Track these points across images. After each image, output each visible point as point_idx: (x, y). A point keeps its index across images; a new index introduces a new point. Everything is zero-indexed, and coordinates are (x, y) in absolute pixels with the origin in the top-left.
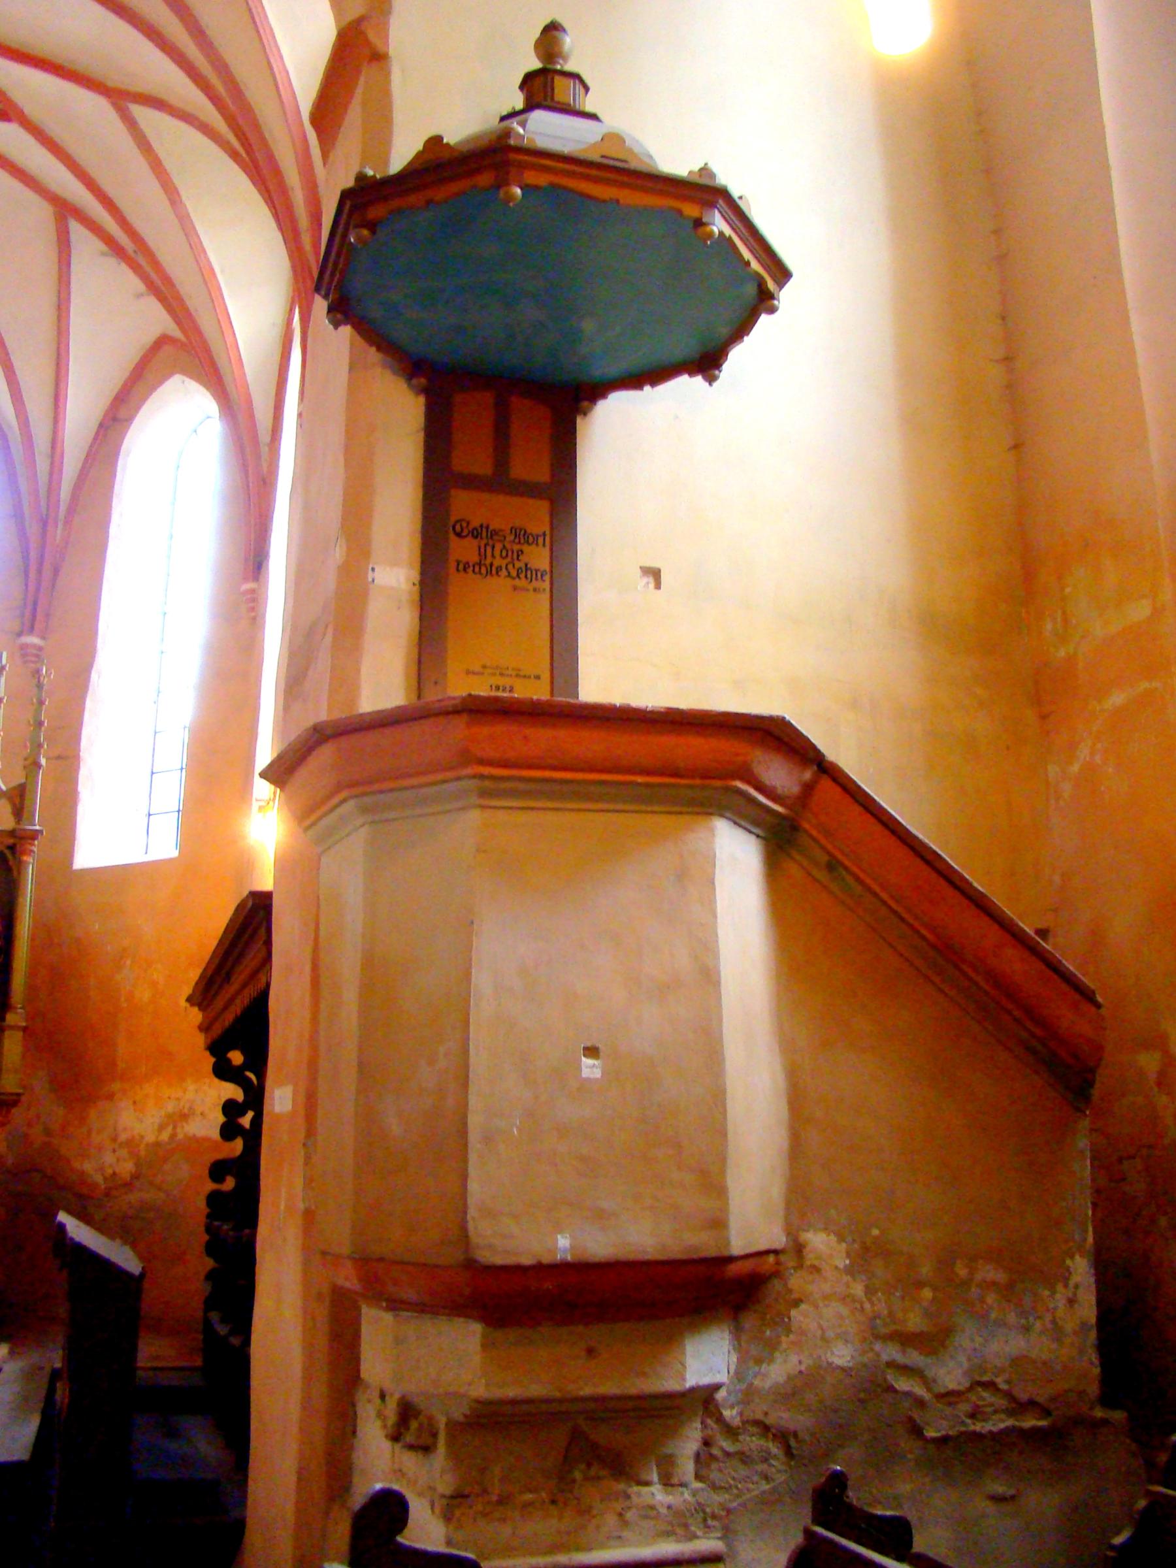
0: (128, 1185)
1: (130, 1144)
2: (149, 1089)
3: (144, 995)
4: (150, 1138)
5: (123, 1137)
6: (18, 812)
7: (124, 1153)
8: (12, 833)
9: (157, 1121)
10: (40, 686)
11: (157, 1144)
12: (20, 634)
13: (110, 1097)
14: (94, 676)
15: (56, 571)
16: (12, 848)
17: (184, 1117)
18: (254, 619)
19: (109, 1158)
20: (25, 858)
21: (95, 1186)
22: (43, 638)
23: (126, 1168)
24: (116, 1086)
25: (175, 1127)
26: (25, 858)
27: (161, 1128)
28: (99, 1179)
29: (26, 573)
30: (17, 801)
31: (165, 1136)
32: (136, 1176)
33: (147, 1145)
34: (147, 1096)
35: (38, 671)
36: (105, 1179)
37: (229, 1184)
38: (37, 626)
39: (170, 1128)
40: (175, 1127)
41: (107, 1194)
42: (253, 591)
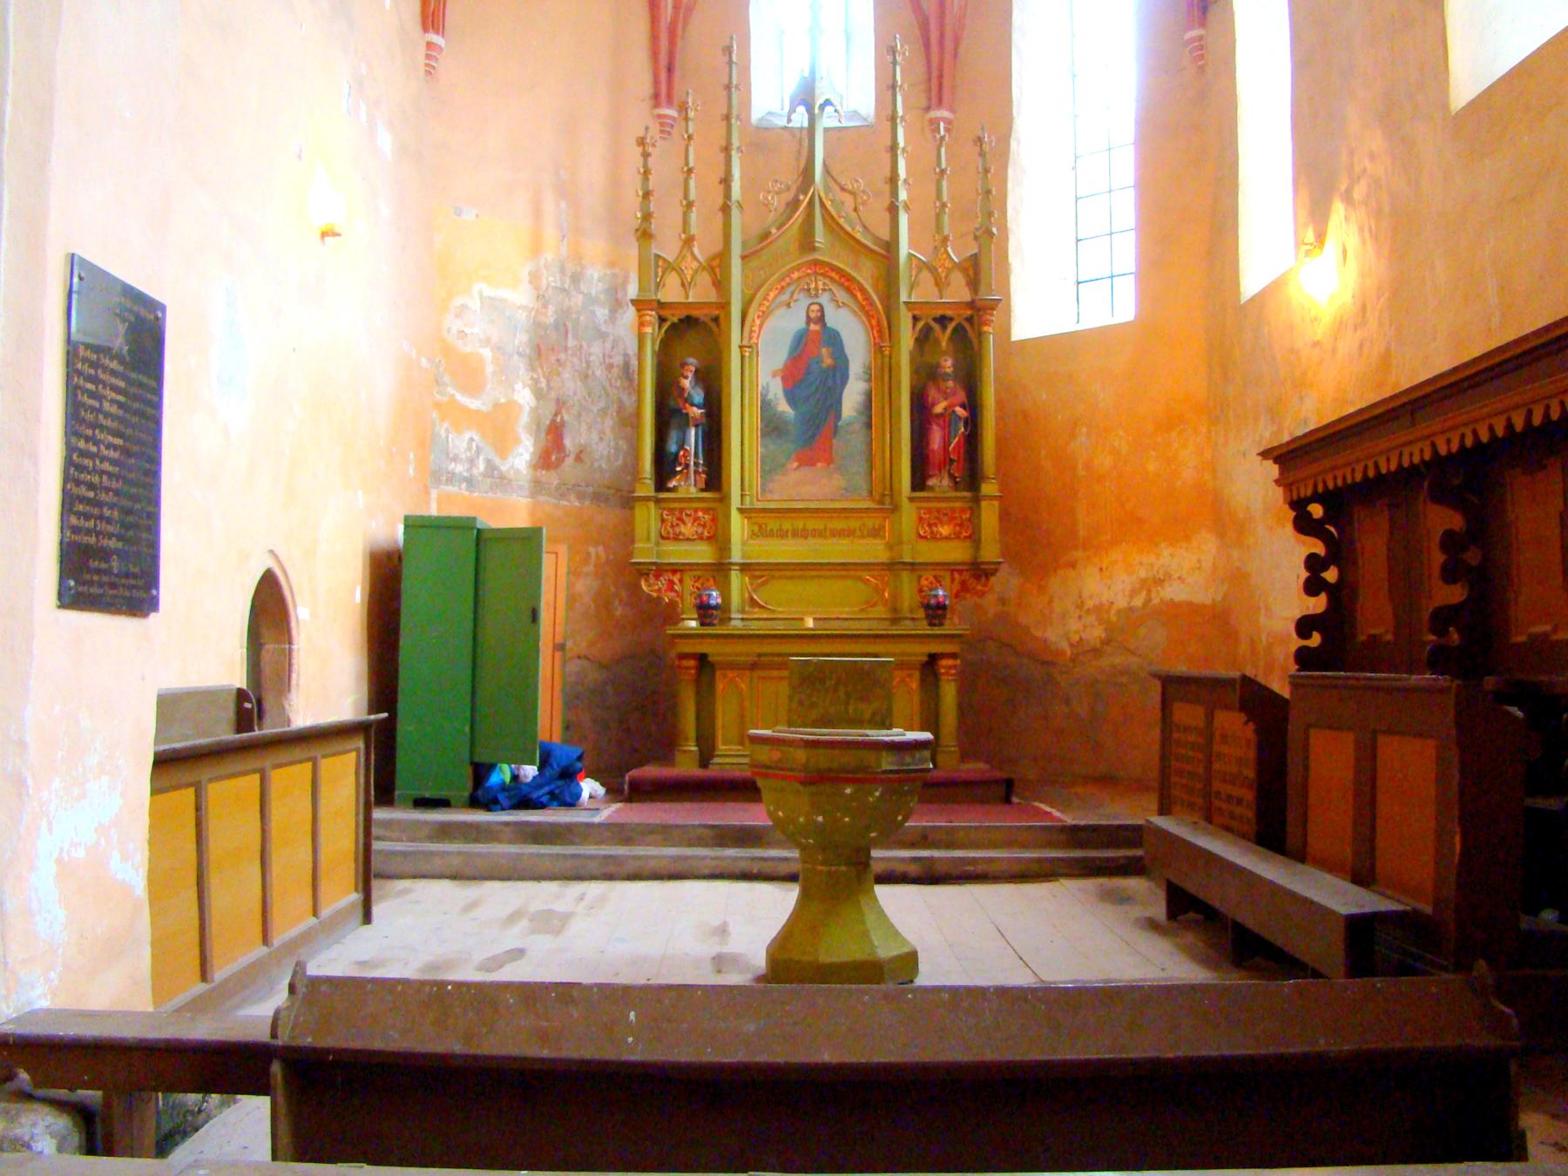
0: (1096, 652)
1: (1098, 609)
2: (1115, 554)
3: (1104, 462)
4: (1122, 603)
5: (1090, 604)
6: (974, 283)
7: (1091, 619)
8: (971, 305)
9: (1129, 588)
10: (982, 154)
11: (1131, 609)
12: (928, 109)
13: (1073, 565)
14: (1013, 143)
15: (957, 40)
16: (969, 320)
17: (1159, 582)
18: (1202, 68)
19: (1074, 625)
20: (985, 328)
21: (1060, 653)
22: (952, 111)
23: (1096, 633)
24: (1079, 554)
26: (985, 328)
27: (1133, 593)
28: (1065, 645)
29: (927, 46)
30: (971, 272)
31: (1138, 602)
32: (1107, 642)
33: (1119, 611)
34: (1114, 563)
35: (980, 140)
36: (1072, 645)
37: (1315, 640)
38: (946, 96)
40: (1149, 591)
41: (1072, 660)
42: (1201, 38)
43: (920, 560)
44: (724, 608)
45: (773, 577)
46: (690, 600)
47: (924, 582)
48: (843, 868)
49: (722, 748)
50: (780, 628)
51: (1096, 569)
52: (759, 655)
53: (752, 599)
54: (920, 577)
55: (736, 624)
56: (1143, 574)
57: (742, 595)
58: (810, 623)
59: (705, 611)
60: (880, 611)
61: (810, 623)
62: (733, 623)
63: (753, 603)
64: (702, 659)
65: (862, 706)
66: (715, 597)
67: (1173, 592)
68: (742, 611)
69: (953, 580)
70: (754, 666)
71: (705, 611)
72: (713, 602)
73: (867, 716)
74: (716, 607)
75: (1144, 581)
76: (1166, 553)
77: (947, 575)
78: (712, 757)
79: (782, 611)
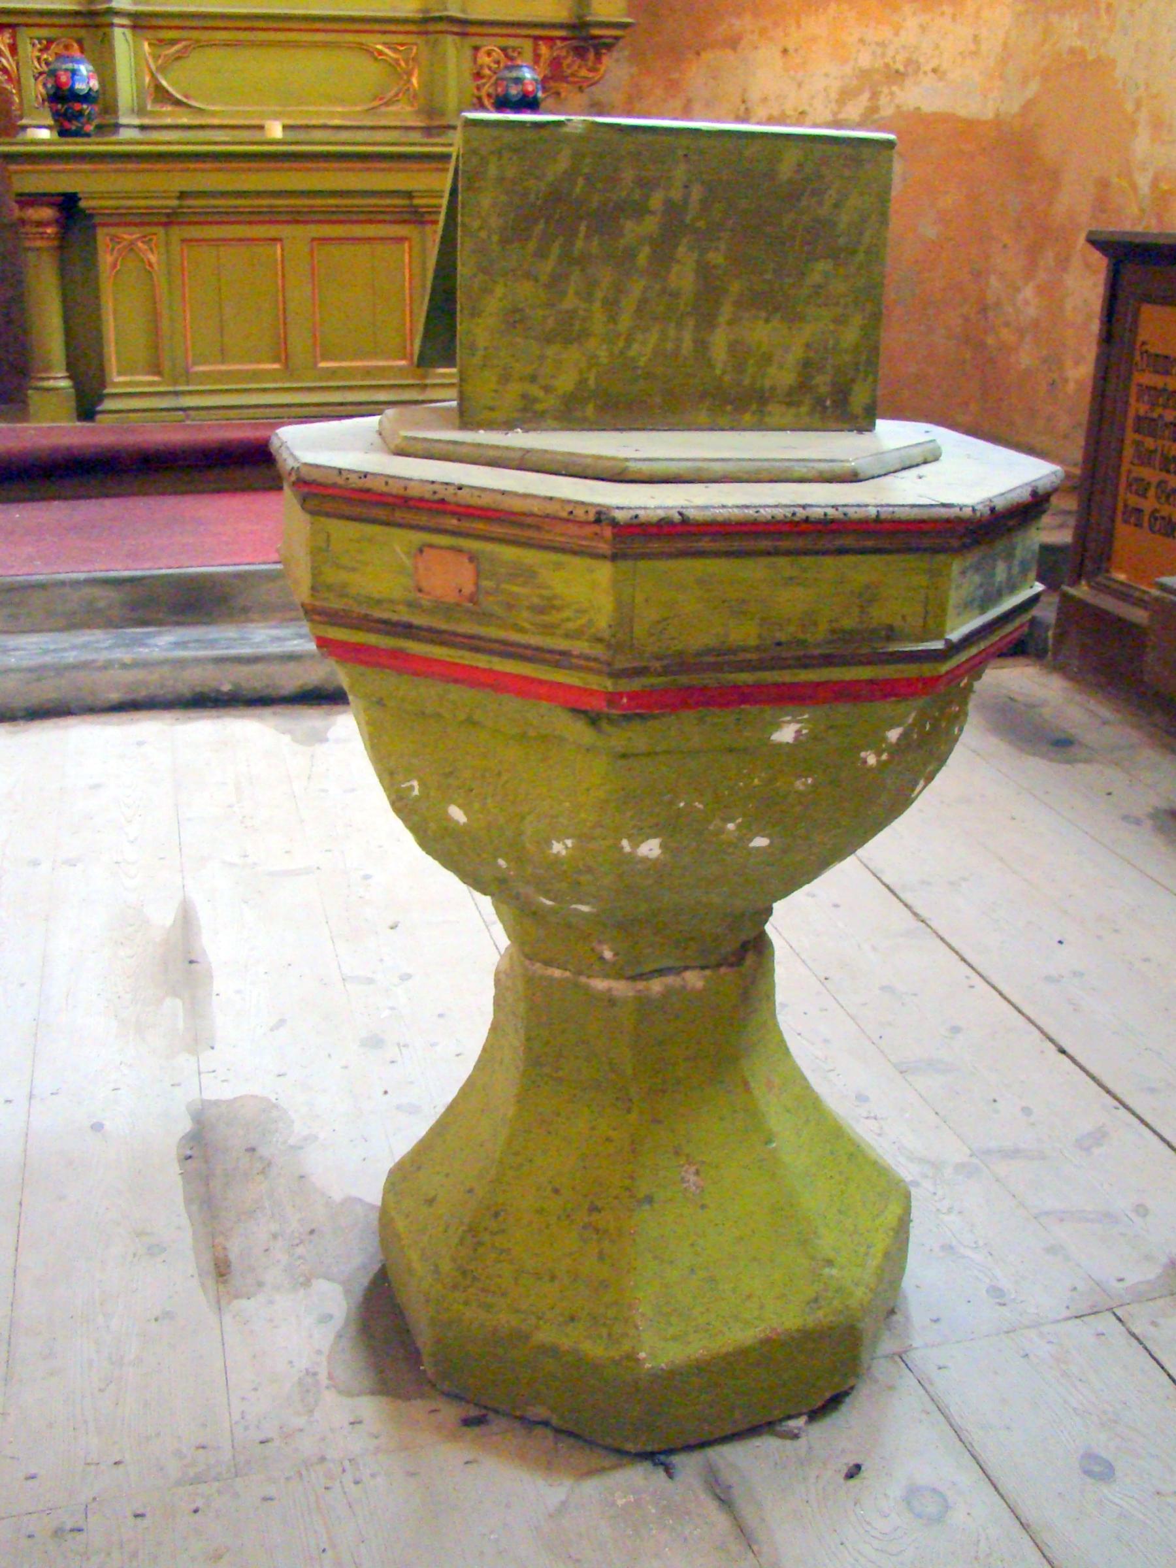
2: (815, 25)
9: (835, 86)
13: (733, 42)
17: (896, 76)
24: (744, 23)
25: (874, 96)
27: (846, 95)
34: (814, 39)
39: (864, 99)
40: (874, 96)
43: (475, 14)
44: (104, 99)
45: (200, 45)
46: (35, 90)
47: (484, 60)
48: (694, 979)
49: (117, 379)
50: (221, 141)
51: (776, 52)
52: (182, 195)
53: (158, 87)
54: (476, 49)
55: (128, 137)
56: (865, 60)
57: (138, 75)
58: (276, 131)
59: (65, 104)
60: (404, 113)
61: (276, 131)
62: (125, 134)
63: (162, 95)
64: (68, 204)
65: (761, 332)
66: (85, 78)
67: (919, 96)
68: (141, 111)
69: (537, 57)
70: (170, 219)
71: (65, 104)
72: (81, 87)
73: (783, 376)
74: (87, 98)
75: (864, 74)
76: (912, 23)
77: (528, 45)
78: (101, 398)
79: (219, 111)
